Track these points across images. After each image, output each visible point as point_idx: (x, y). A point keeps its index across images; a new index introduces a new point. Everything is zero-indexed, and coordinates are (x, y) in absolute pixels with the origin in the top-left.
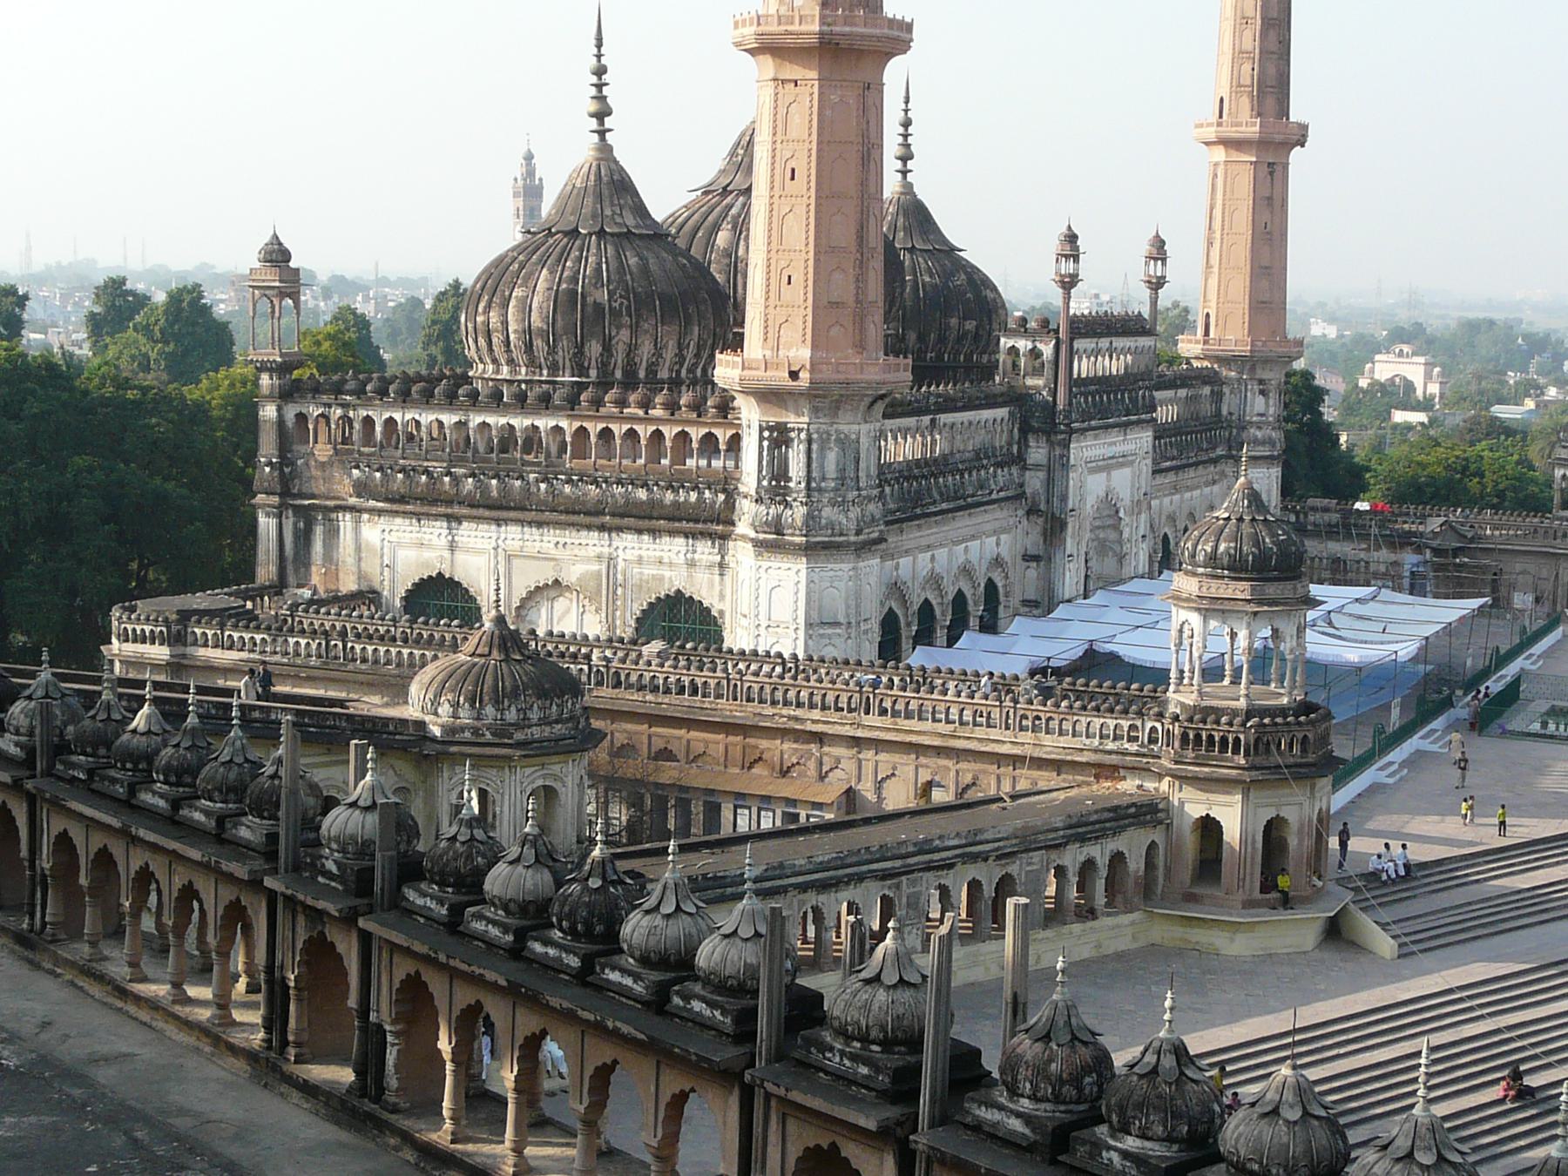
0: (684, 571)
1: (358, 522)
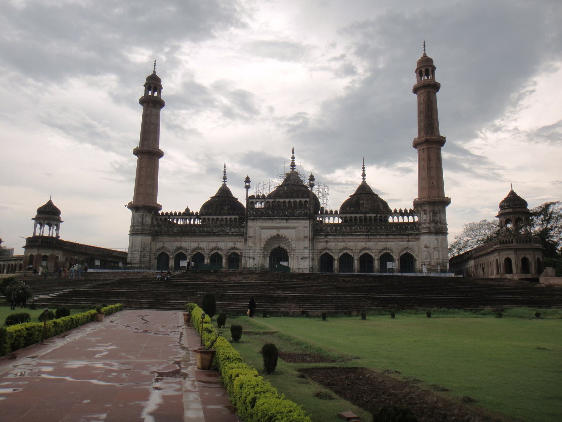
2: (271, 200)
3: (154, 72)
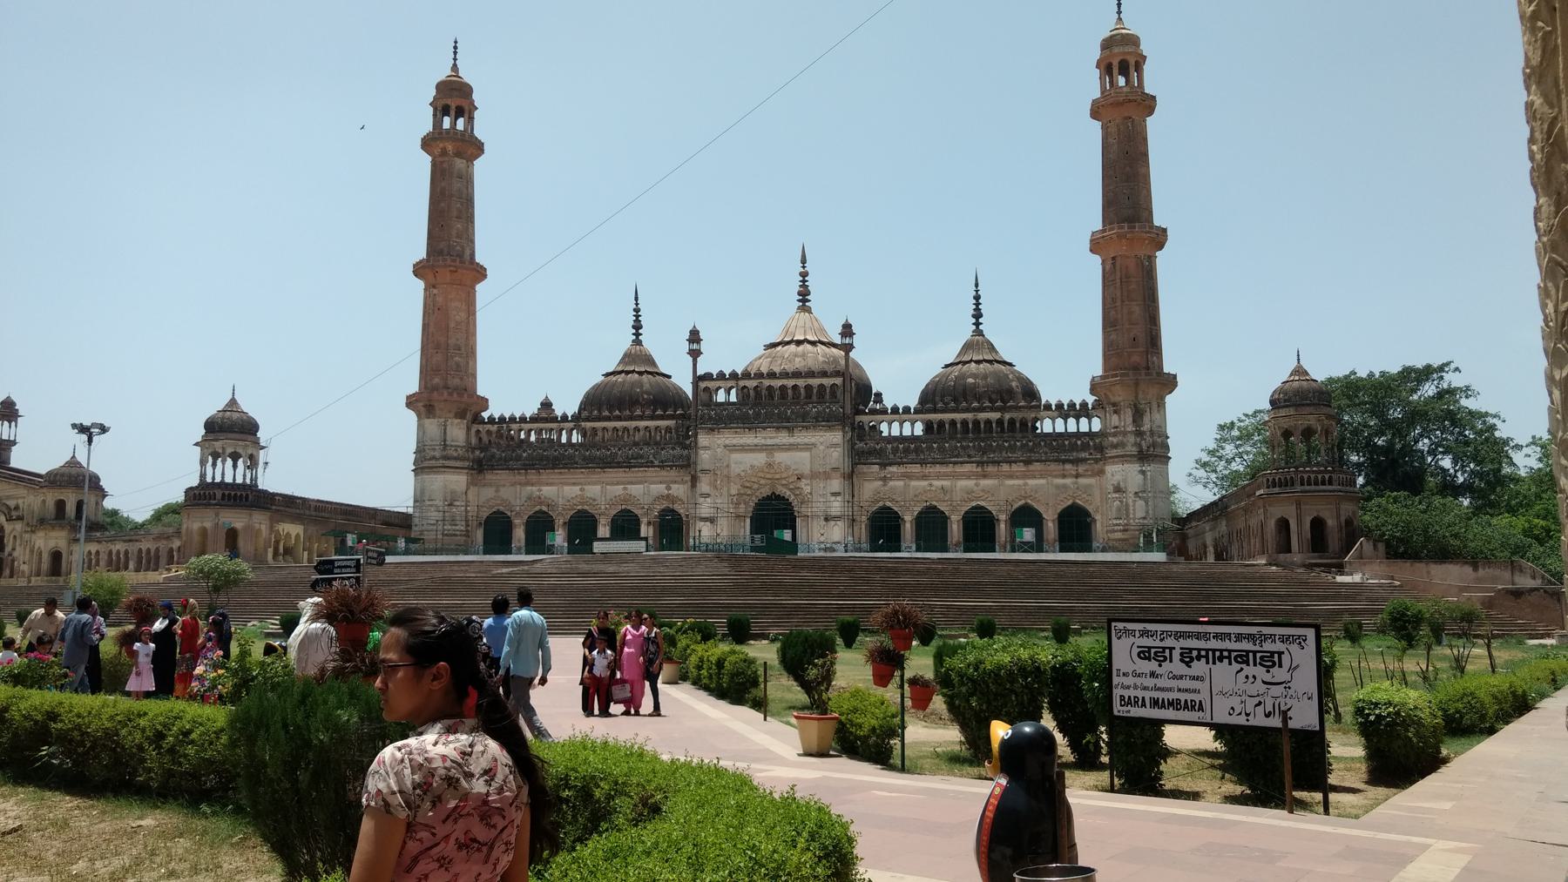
2: (752, 384)
3: (455, 67)
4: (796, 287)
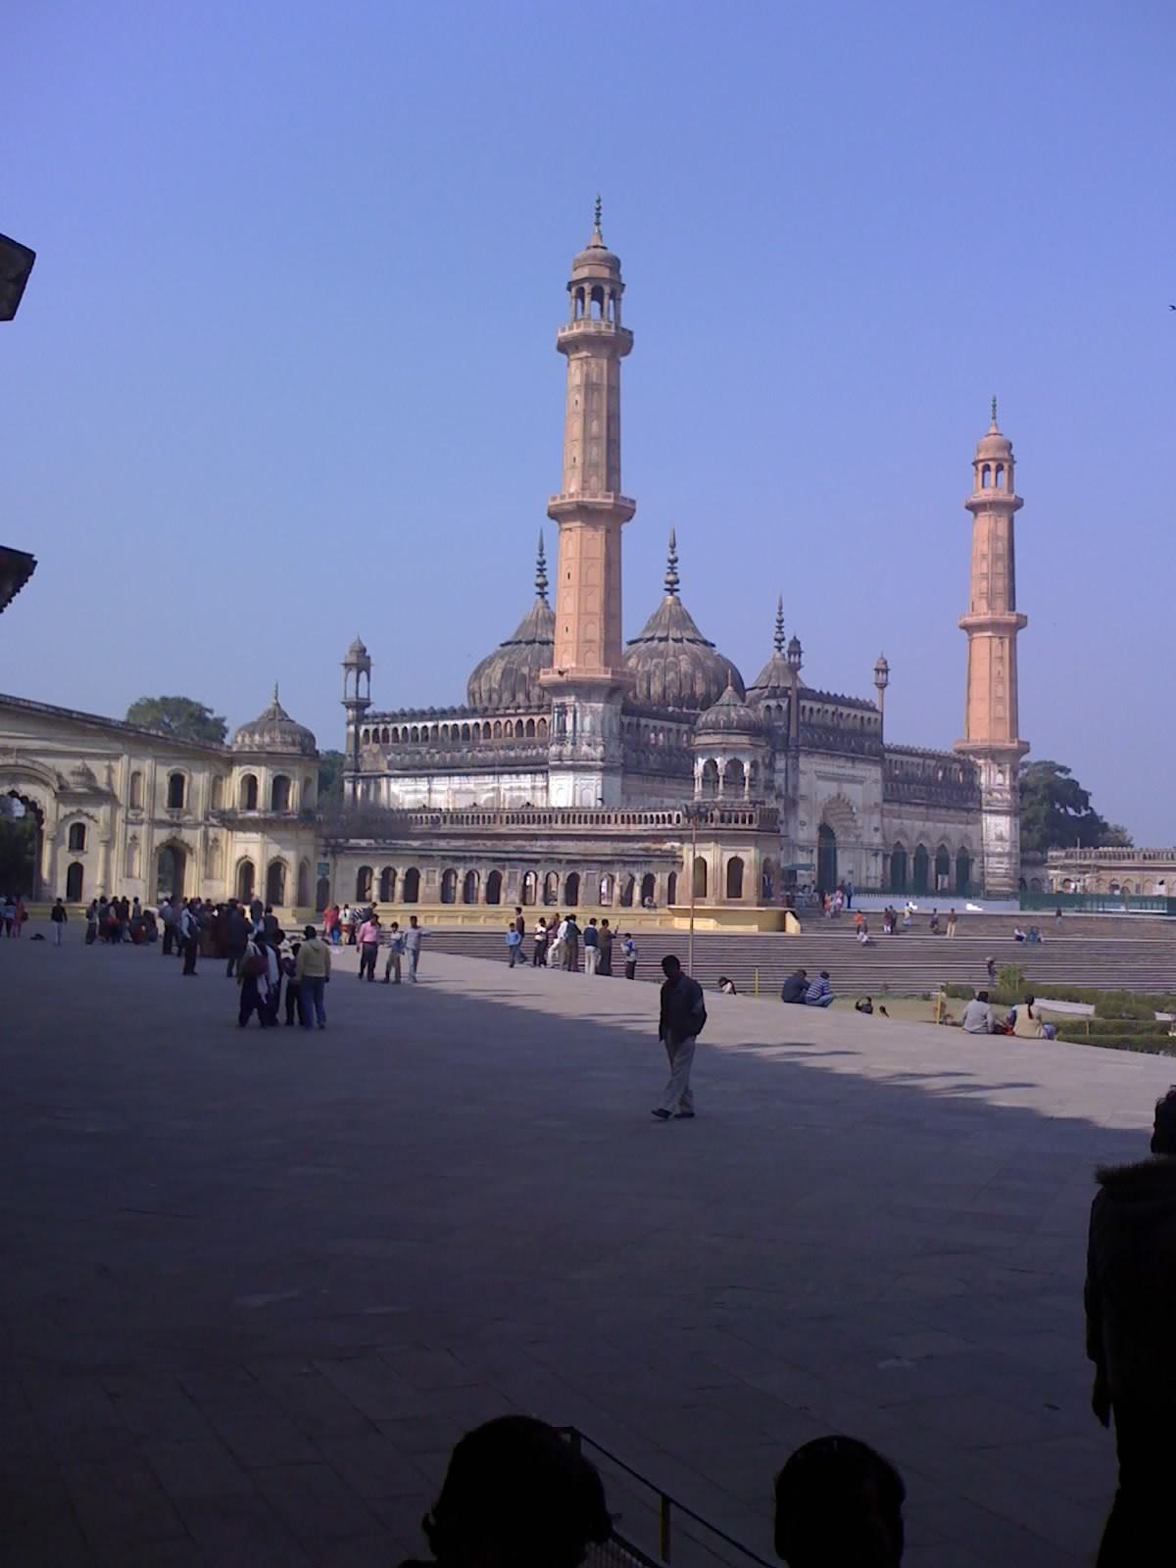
0: (530, 793)
1: (389, 783)
4: (663, 575)
